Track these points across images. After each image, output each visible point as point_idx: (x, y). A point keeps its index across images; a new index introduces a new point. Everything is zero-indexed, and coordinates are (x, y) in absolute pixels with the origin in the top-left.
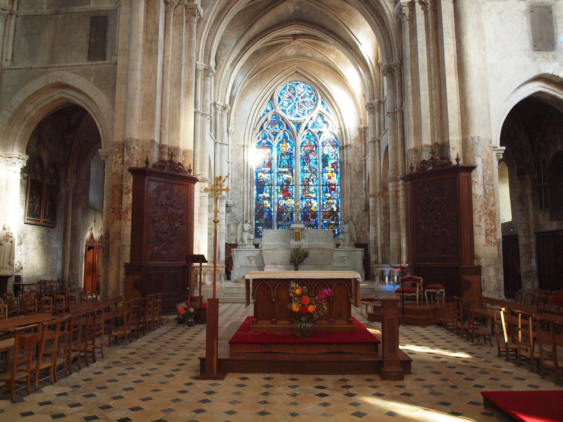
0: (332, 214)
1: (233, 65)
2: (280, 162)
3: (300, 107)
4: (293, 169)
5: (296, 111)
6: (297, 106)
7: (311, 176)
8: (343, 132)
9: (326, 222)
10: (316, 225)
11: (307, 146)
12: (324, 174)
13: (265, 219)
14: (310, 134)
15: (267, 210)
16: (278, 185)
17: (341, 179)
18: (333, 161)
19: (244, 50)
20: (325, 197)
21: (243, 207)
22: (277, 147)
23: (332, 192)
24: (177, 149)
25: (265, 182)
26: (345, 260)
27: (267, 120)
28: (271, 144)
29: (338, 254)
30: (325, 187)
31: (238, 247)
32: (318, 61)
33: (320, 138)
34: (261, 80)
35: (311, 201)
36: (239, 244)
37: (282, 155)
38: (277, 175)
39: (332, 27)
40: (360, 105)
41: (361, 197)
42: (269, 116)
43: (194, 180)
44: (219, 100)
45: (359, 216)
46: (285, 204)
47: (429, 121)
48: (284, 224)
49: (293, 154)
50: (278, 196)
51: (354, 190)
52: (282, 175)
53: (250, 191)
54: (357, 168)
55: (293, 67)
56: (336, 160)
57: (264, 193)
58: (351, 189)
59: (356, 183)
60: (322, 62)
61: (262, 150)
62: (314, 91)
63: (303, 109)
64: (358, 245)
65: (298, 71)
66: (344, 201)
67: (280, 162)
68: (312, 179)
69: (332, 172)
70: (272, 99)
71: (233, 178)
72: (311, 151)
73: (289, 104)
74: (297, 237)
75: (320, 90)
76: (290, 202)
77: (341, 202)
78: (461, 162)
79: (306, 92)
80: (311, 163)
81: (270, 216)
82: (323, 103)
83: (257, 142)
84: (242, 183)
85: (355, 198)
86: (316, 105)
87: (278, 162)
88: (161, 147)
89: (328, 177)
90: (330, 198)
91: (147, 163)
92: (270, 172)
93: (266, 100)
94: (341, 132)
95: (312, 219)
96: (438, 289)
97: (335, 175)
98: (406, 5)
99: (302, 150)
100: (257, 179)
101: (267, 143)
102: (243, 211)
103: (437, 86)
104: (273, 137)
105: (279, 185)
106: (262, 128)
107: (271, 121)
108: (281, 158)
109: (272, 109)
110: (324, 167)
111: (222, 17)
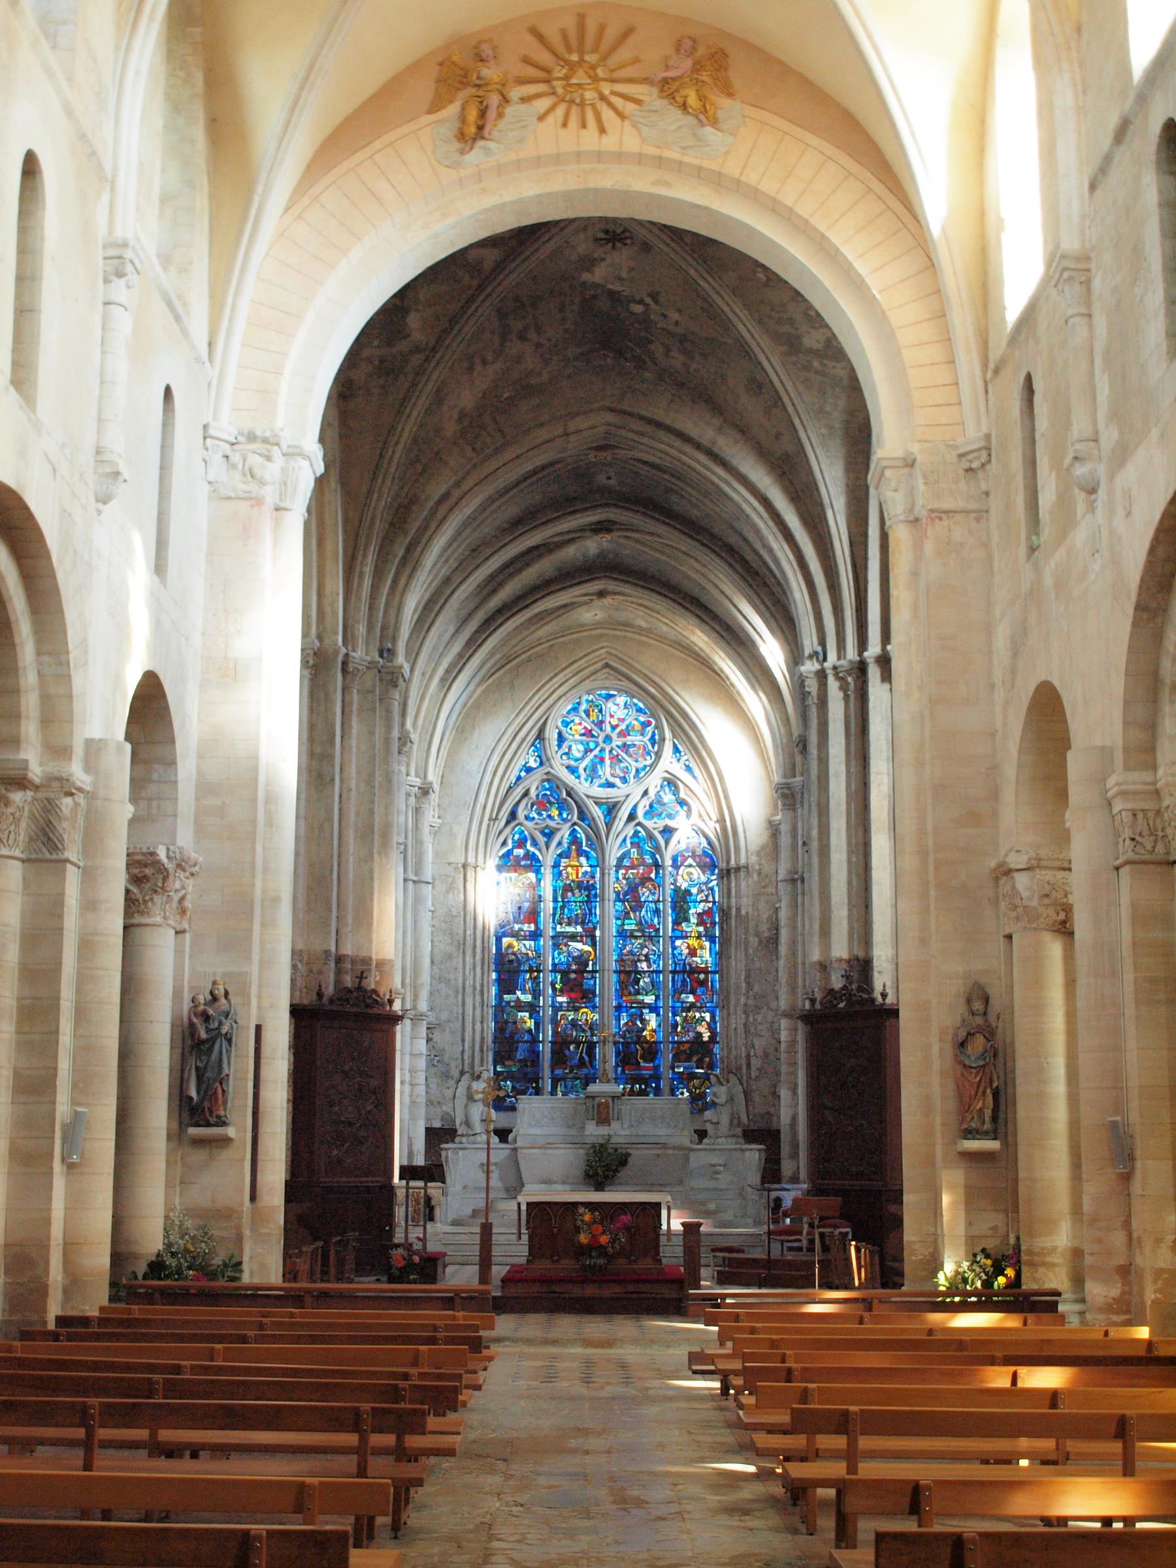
0: (698, 1050)
1: (447, 681)
2: (562, 908)
3: (616, 759)
4: (595, 928)
5: (606, 771)
6: (607, 756)
7: (643, 947)
8: (728, 832)
9: (681, 1070)
10: (657, 1077)
11: (633, 867)
12: (678, 943)
13: (520, 1061)
14: (643, 833)
15: (526, 1037)
16: (554, 971)
17: (721, 955)
18: (701, 908)
19: (474, 644)
20: (678, 1005)
21: (464, 1030)
22: (554, 867)
23: (699, 992)
24: (367, 961)
25: (519, 963)
26: (719, 1173)
27: (526, 794)
28: (539, 861)
29: (701, 1158)
30: (679, 978)
31: (457, 1139)
32: (662, 639)
33: (667, 843)
34: (512, 687)
35: (642, 1014)
36: (459, 1132)
37: (567, 888)
38: (554, 945)
39: (696, 592)
40: (773, 760)
41: (773, 1005)
42: (533, 784)
43: (396, 1019)
44: (413, 773)
45: (766, 1055)
46: (574, 1024)
47: (844, 913)
48: (571, 1076)
49: (593, 887)
50: (553, 998)
51: (757, 988)
52: (566, 945)
53: (482, 985)
54: (764, 927)
55: (597, 653)
56: (710, 905)
57: (519, 993)
58: (748, 983)
59: (760, 969)
60: (675, 642)
61: (514, 875)
62: (653, 716)
63: (622, 765)
64: (750, 1136)
65: (611, 663)
66: (729, 1014)
67: (562, 908)
68: (646, 956)
69: (699, 937)
70: (540, 736)
71: (436, 951)
72: (645, 880)
73: (587, 751)
74: (603, 1113)
75: (668, 714)
76: (587, 1015)
77: (722, 1018)
78: (889, 1000)
79: (634, 720)
80: (643, 913)
81: (534, 1057)
82: (676, 749)
83: (501, 854)
84: (461, 965)
85: (758, 1008)
86: (658, 755)
87: (555, 909)
88: (339, 959)
89: (686, 951)
90: (692, 1006)
91: (320, 995)
92: (535, 935)
93: (524, 740)
94: (724, 829)
95: (645, 1061)
96: (835, 1227)
97: (707, 944)
98: (812, 675)
99: (621, 877)
100: (500, 954)
101: (529, 856)
102: (463, 1040)
103: (861, 848)
104: (542, 840)
105: (559, 971)
106: (513, 815)
107: (537, 796)
108: (563, 897)
109: (541, 764)
110: (677, 923)
111: (433, 615)
